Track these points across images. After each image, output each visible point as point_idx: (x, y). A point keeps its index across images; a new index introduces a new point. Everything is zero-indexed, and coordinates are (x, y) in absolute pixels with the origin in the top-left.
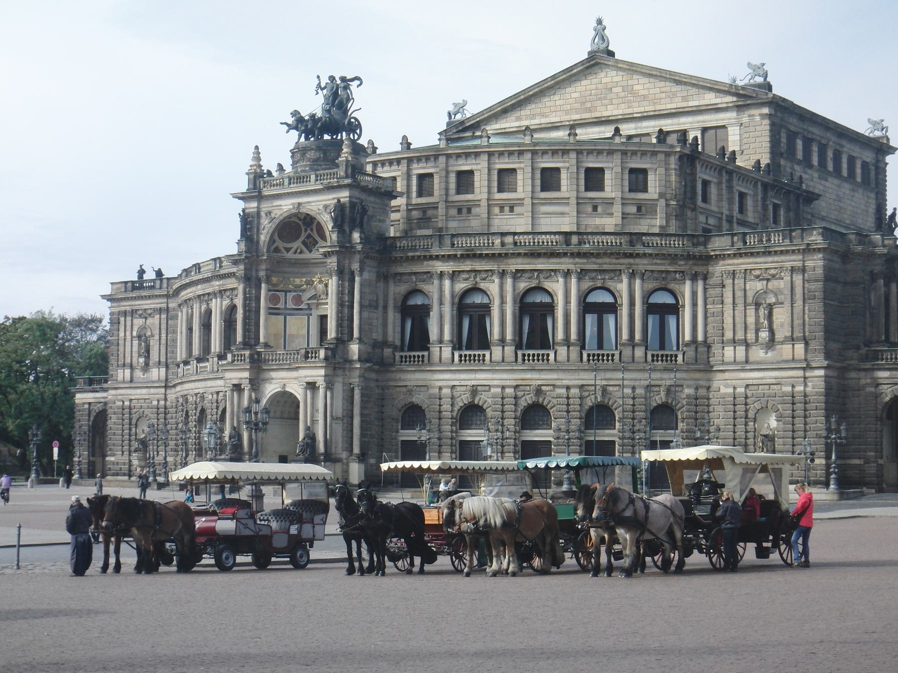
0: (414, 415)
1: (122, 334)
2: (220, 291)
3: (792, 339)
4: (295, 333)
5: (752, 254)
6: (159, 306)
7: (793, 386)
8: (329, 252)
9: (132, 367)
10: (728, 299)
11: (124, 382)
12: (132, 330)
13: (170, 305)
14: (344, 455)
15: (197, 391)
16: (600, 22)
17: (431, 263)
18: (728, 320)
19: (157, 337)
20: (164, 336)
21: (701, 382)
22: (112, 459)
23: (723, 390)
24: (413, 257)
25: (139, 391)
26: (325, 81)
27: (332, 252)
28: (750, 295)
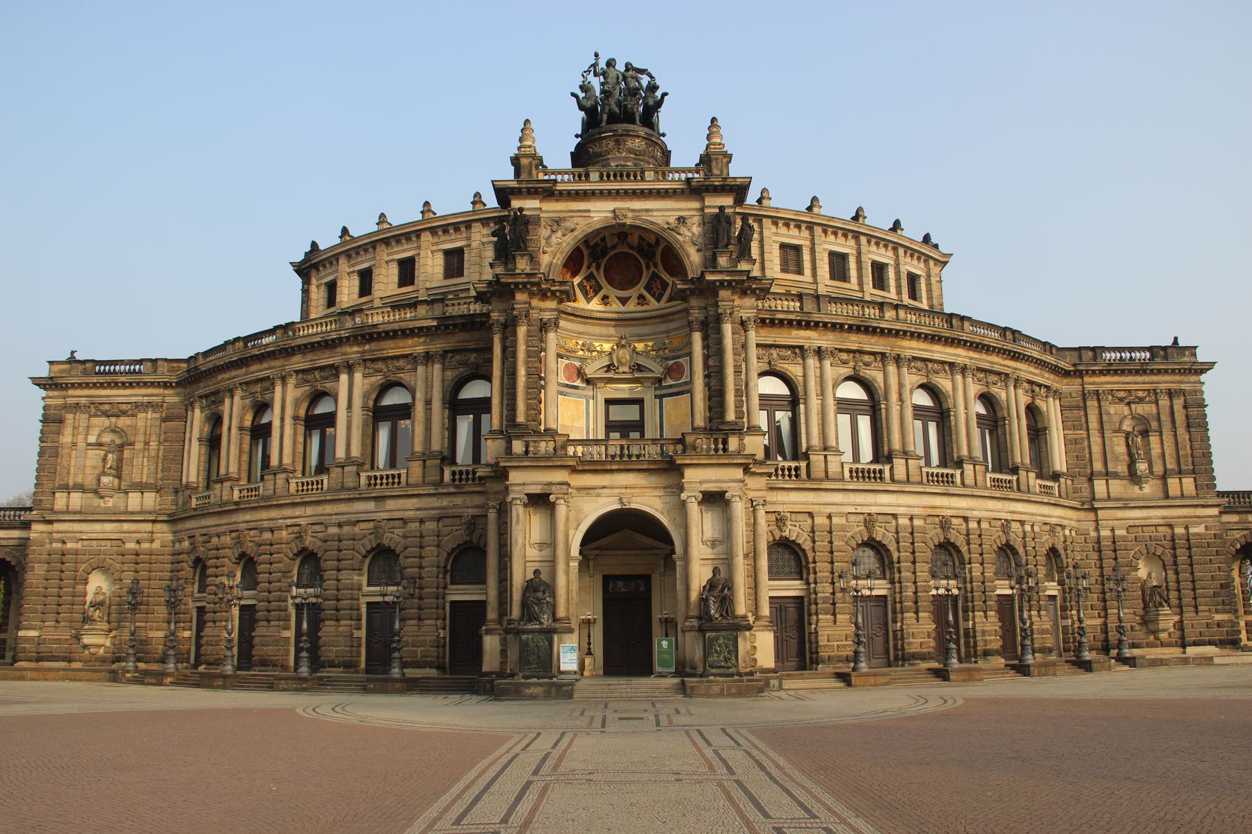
0: (789, 555)
1: (66, 438)
2: (365, 361)
4: (569, 424)
5: (1123, 372)
8: (722, 282)
9: (80, 488)
10: (1093, 424)
11: (68, 512)
12: (87, 435)
13: (168, 399)
14: (751, 619)
15: (289, 522)
18: (1096, 449)
19: (139, 446)
20: (153, 445)
21: (1074, 524)
24: (781, 321)
25: (98, 527)
26: (602, 65)
27: (730, 282)
28: (1116, 419)
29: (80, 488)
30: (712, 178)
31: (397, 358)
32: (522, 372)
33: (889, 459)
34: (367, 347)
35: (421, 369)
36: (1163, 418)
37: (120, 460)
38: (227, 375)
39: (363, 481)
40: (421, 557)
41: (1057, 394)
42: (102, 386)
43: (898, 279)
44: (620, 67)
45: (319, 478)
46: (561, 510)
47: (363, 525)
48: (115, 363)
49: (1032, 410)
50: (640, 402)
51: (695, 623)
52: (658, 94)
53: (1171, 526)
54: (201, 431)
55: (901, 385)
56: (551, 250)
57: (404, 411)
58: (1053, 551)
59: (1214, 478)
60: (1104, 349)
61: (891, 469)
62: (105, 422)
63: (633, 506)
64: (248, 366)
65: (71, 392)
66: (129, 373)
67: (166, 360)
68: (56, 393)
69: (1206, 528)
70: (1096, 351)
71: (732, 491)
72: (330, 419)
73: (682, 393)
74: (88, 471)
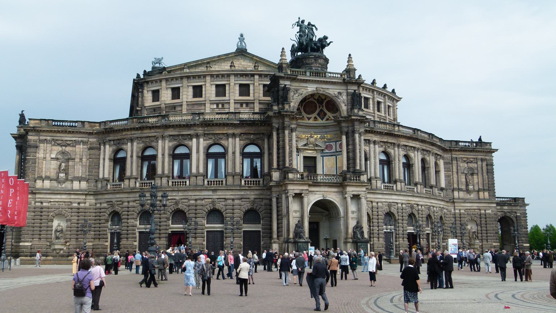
1: (40, 155)
3: (484, 190)
5: (466, 151)
6: (80, 139)
7: (485, 211)
8: (357, 119)
9: (48, 178)
10: (455, 170)
16: (242, 35)
17: (370, 135)
20: (84, 160)
21: (447, 207)
22: (26, 244)
23: (453, 211)
25: (59, 196)
27: (359, 119)
28: (462, 168)
29: (48, 178)
30: (349, 78)
31: (219, 134)
32: (287, 148)
33: (395, 182)
34: (206, 129)
35: (230, 140)
36: (479, 169)
37: (66, 166)
38: (129, 133)
39: (206, 182)
40: (233, 213)
41: (443, 158)
42: (59, 132)
43: (385, 108)
44: (306, 23)
45: (184, 180)
46: (305, 200)
47: (206, 200)
48: (63, 121)
49: (436, 164)
50: (314, 158)
51: (351, 240)
52: (328, 41)
53: (480, 210)
54: (110, 156)
55: (399, 155)
56: (294, 101)
57: (223, 155)
58: (441, 217)
59: (495, 193)
60: (460, 141)
61: (396, 186)
62: (60, 149)
63: (327, 198)
64: (143, 130)
65: (41, 134)
66: (70, 126)
67: (89, 122)
68: (34, 134)
69: (492, 211)
70: (457, 142)
71: (362, 194)
72: (188, 156)
73: (332, 156)
74: (52, 171)
